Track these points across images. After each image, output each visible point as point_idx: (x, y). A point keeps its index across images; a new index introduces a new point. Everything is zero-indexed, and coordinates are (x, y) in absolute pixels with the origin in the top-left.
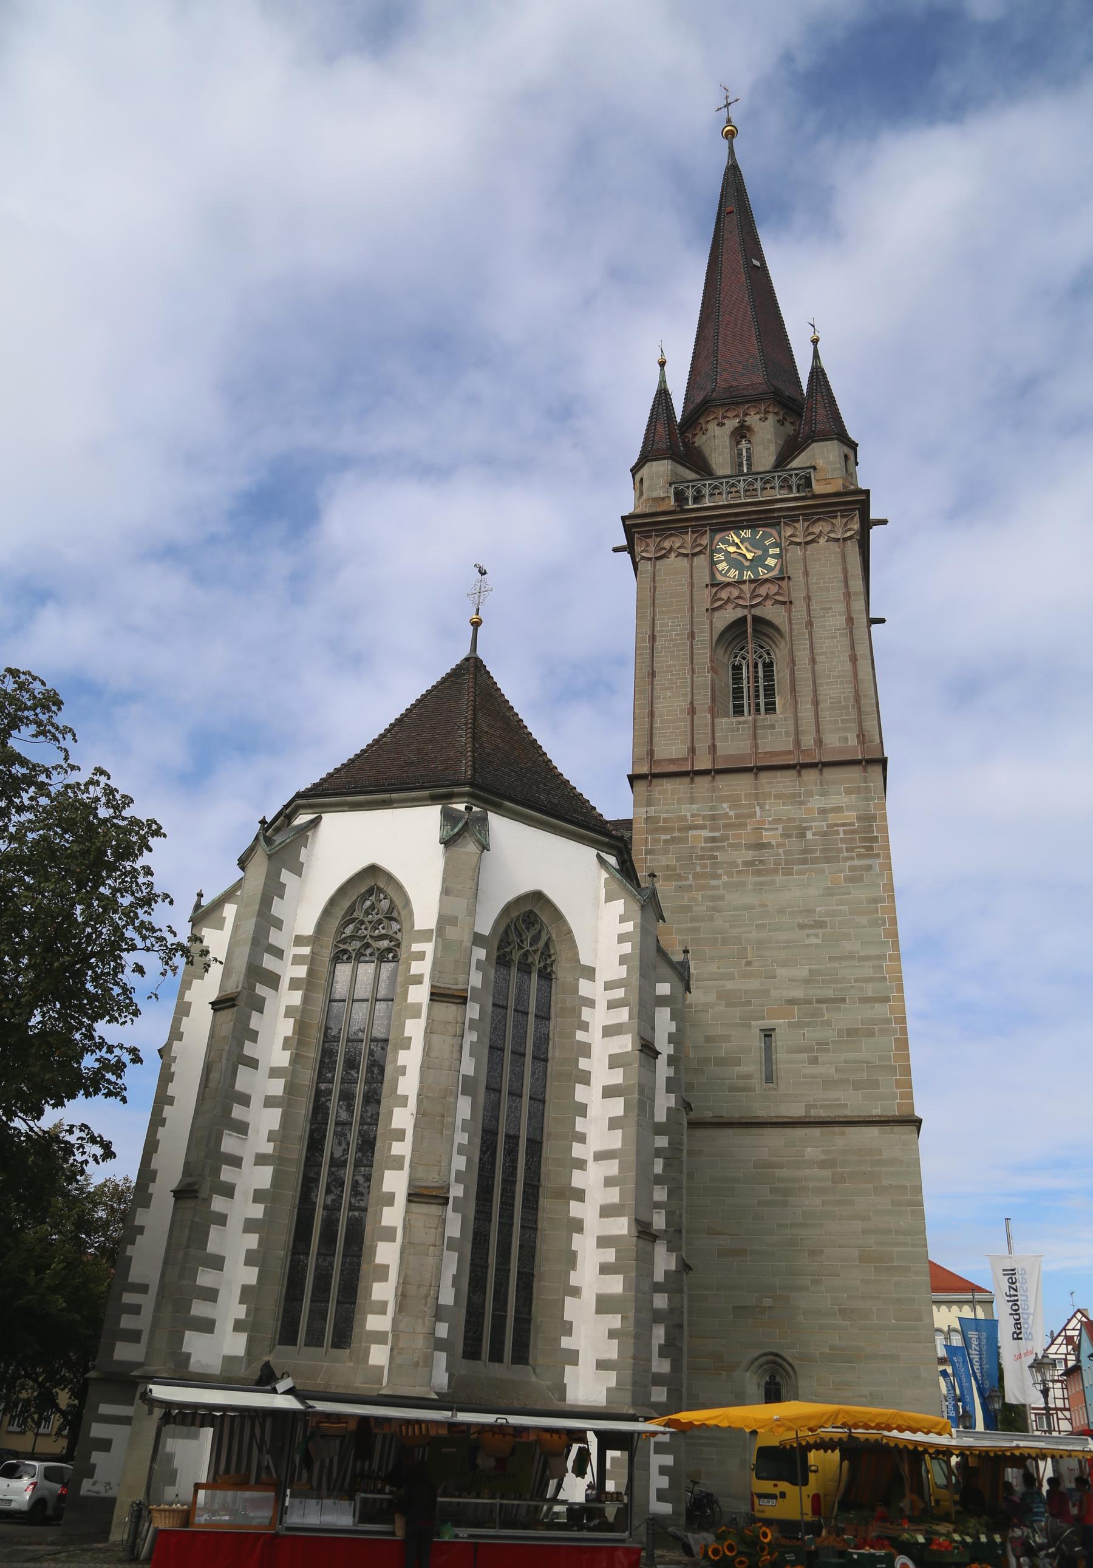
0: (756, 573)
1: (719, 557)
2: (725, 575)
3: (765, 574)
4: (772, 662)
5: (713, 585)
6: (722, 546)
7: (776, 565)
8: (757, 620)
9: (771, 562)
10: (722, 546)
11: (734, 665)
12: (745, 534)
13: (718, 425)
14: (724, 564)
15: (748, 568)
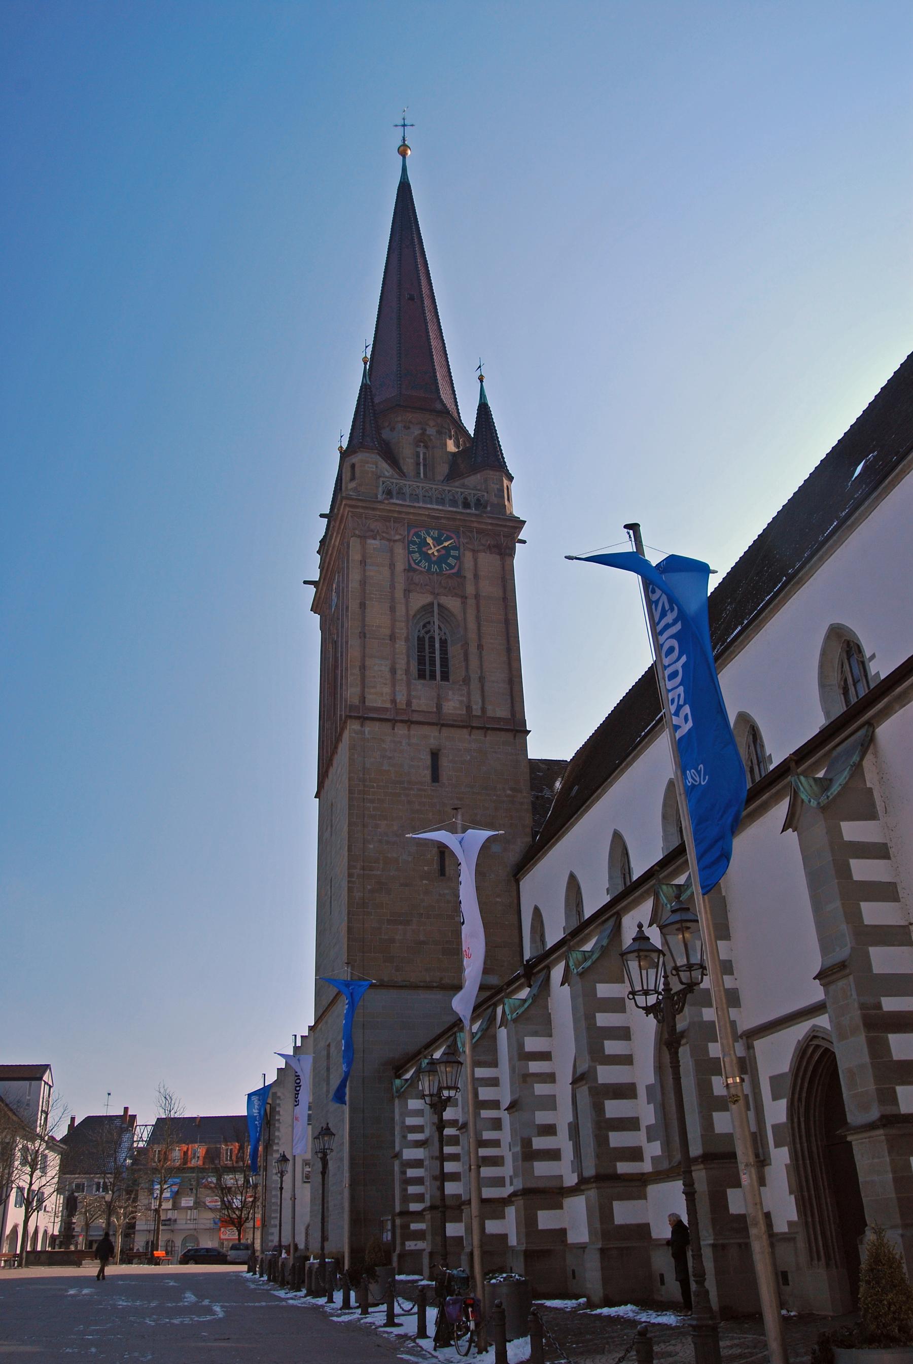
0: (440, 568)
1: (413, 548)
2: (417, 564)
3: (447, 570)
4: (446, 639)
5: (408, 571)
6: (417, 540)
7: (455, 564)
8: (439, 605)
9: (451, 561)
10: (417, 540)
11: (418, 637)
12: (434, 533)
13: (405, 427)
14: (417, 555)
15: (435, 563)
